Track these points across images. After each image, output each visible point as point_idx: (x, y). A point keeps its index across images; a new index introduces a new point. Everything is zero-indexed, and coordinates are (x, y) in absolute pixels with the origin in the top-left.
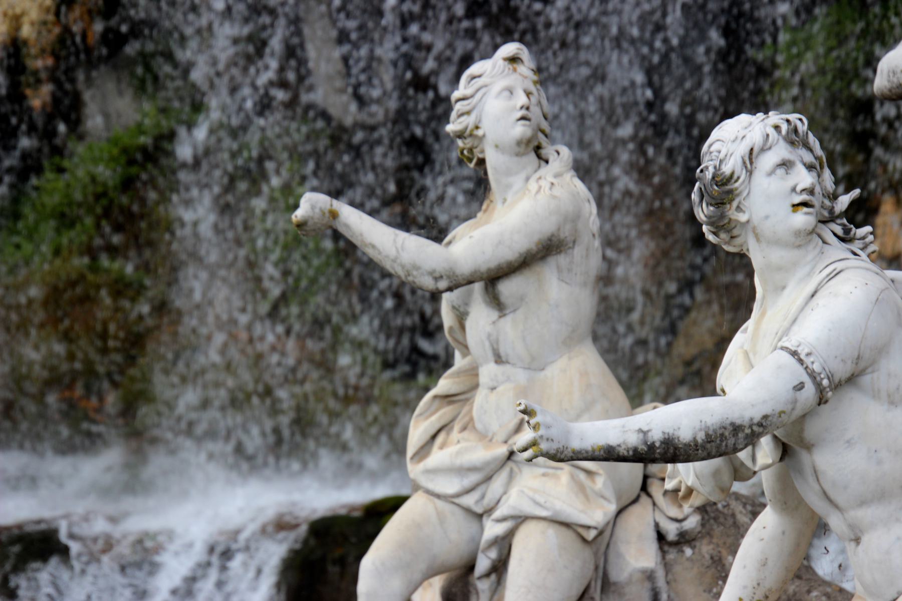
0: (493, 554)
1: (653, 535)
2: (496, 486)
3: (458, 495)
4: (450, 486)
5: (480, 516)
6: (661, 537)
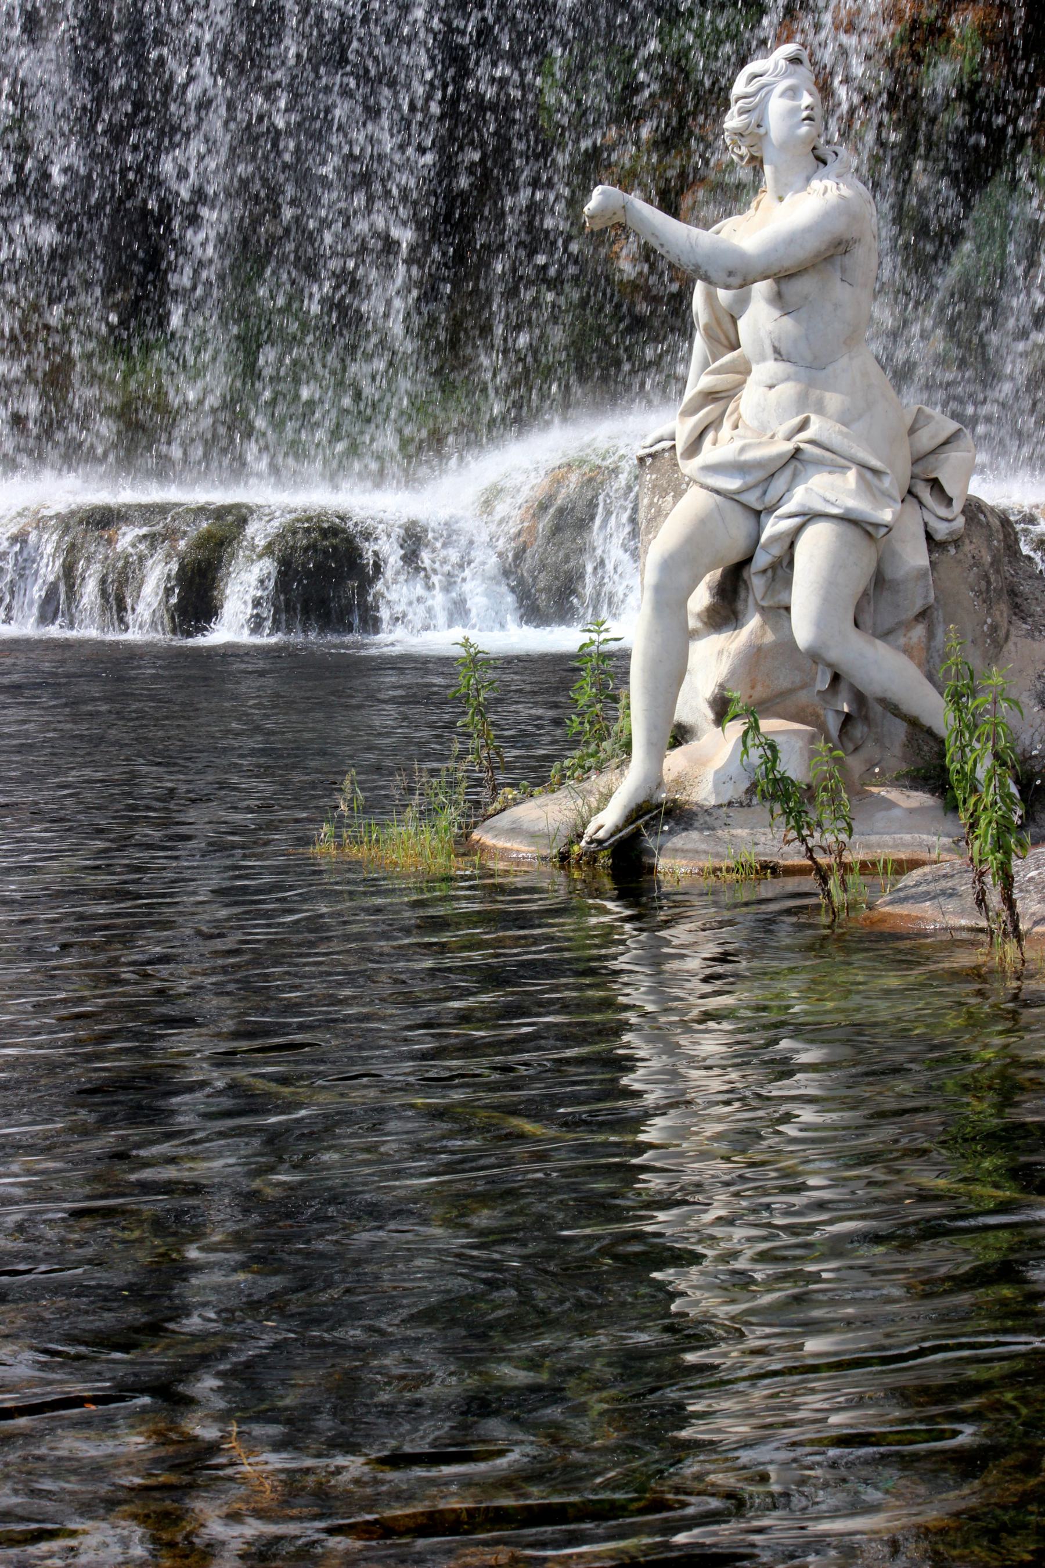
0: (776, 551)
1: (923, 536)
2: (779, 484)
3: (739, 492)
4: (732, 484)
5: (758, 514)
6: (929, 537)
